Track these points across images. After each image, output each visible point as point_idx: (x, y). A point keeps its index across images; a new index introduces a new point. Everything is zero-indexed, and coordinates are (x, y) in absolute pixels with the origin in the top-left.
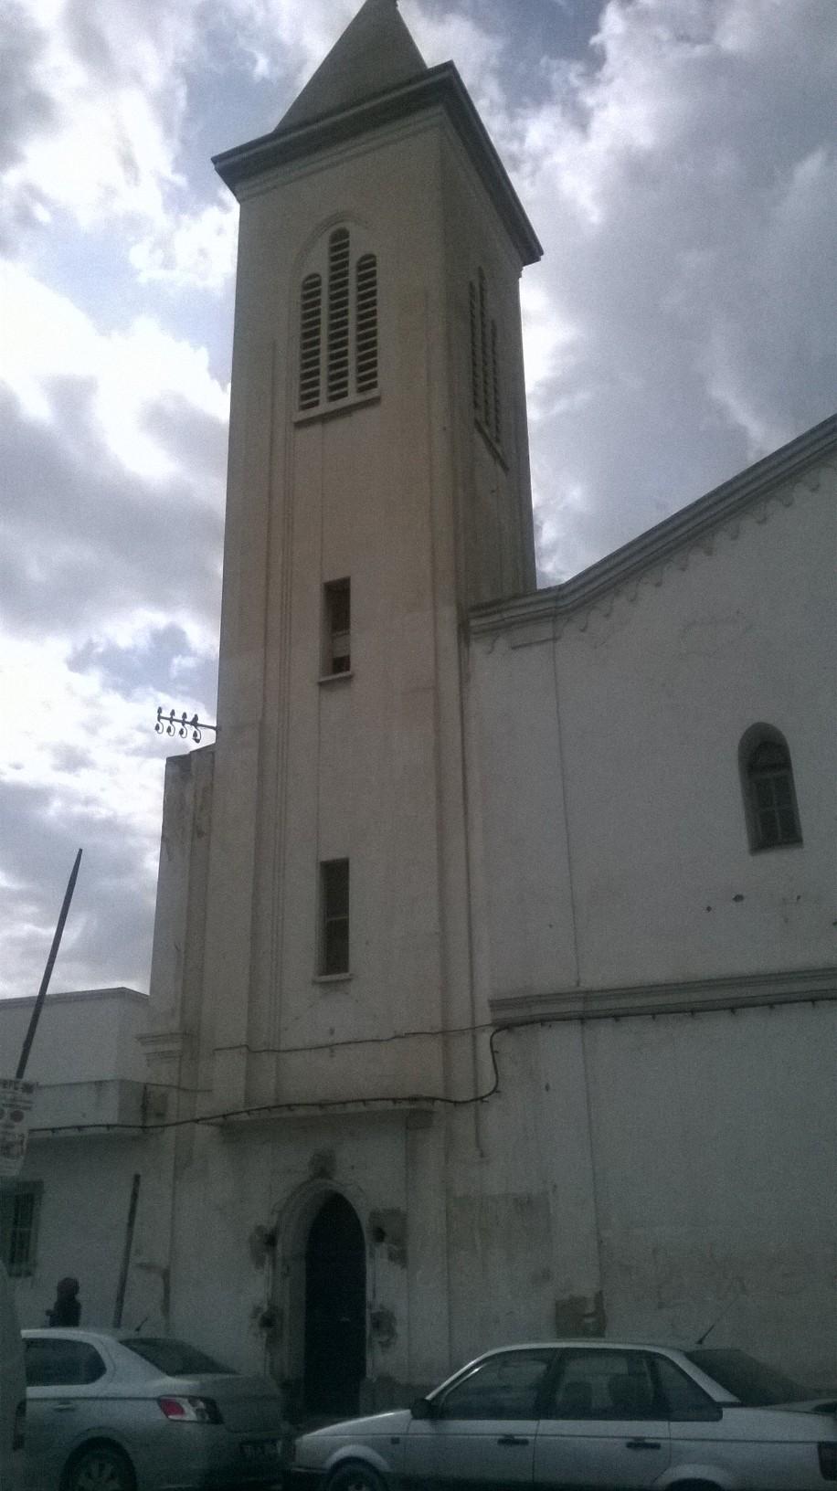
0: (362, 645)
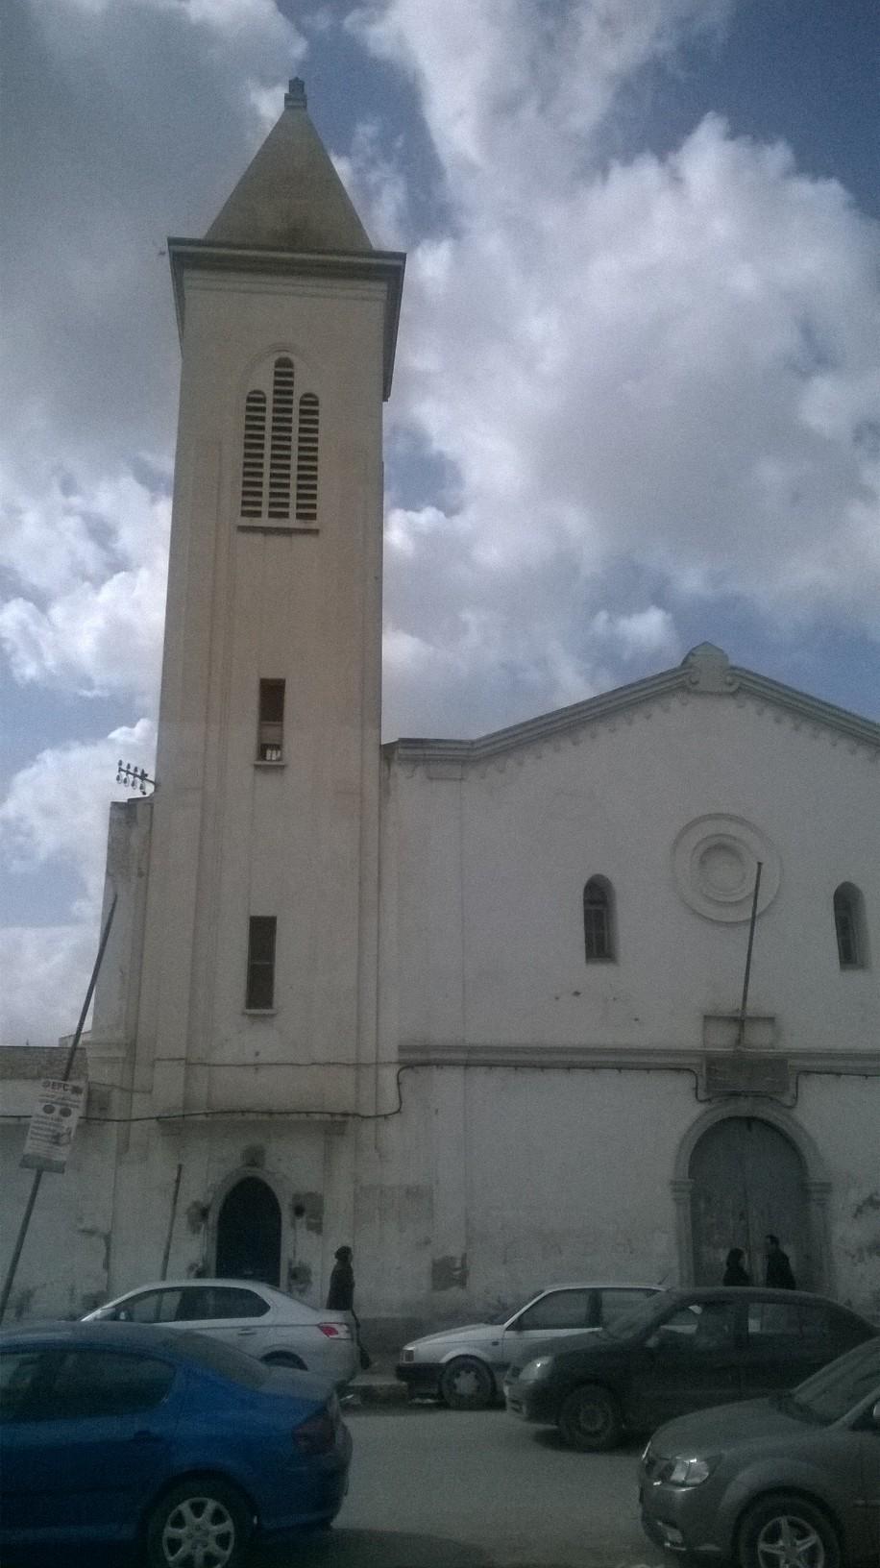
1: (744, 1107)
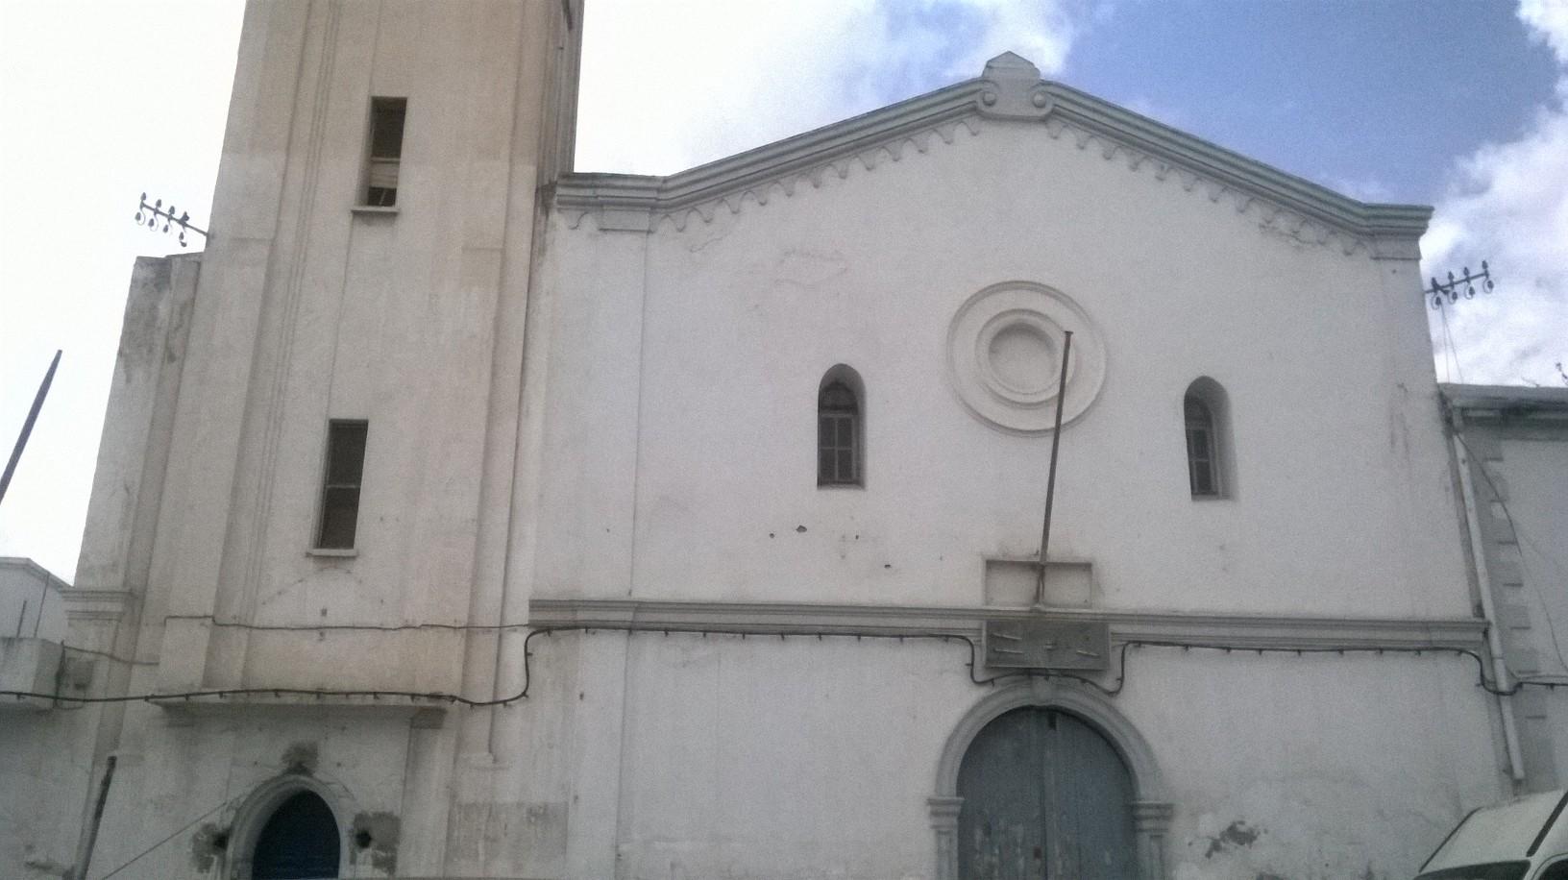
0: (413, 179)
1: (1043, 693)
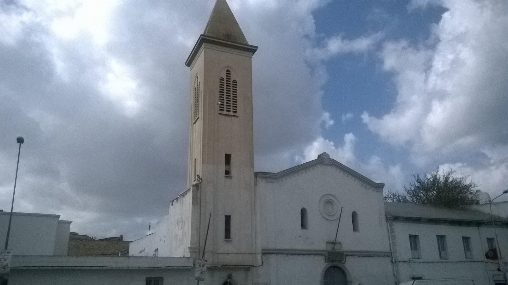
0: (234, 171)
1: (335, 264)
